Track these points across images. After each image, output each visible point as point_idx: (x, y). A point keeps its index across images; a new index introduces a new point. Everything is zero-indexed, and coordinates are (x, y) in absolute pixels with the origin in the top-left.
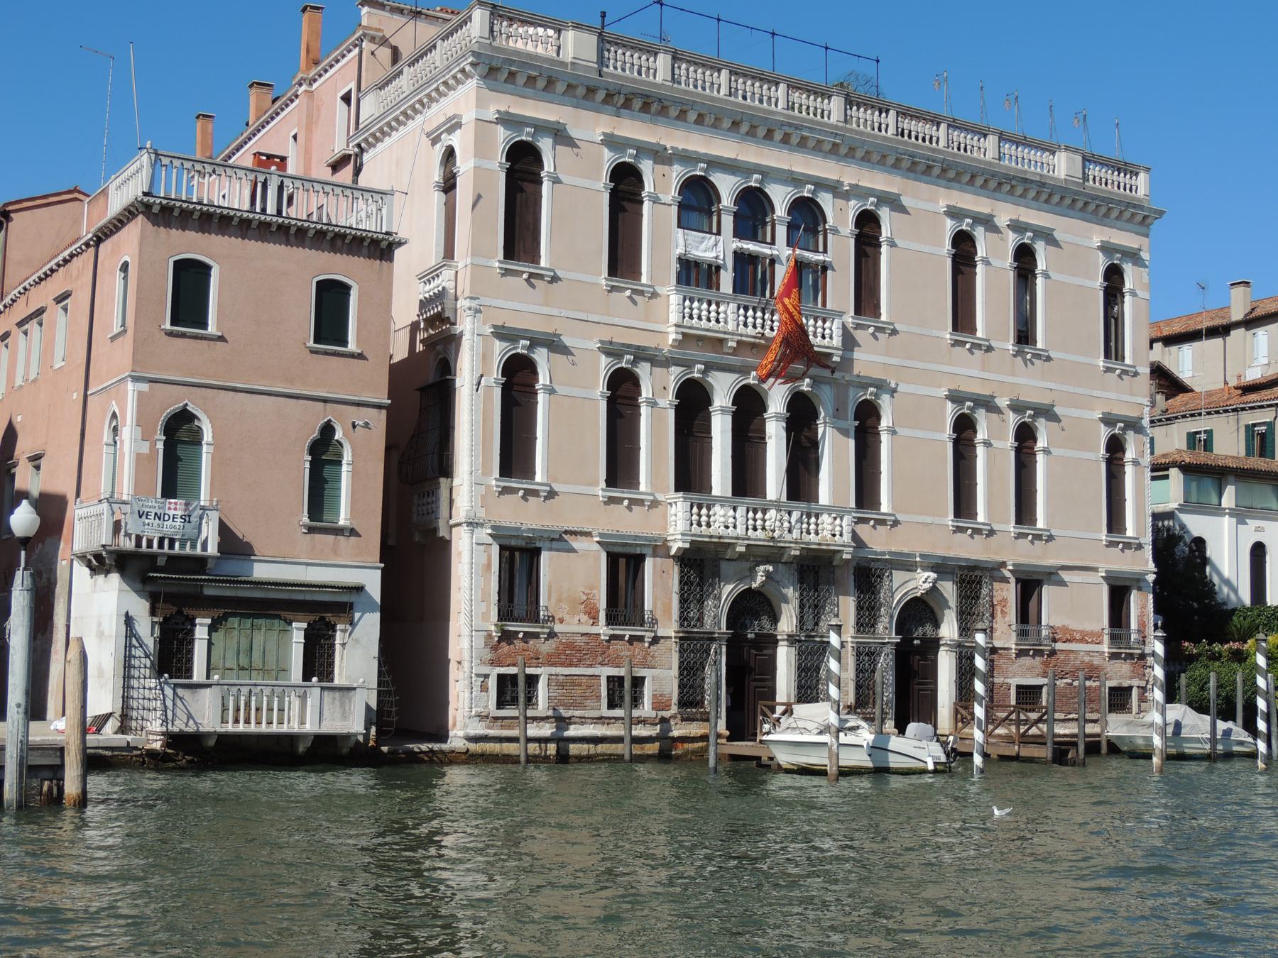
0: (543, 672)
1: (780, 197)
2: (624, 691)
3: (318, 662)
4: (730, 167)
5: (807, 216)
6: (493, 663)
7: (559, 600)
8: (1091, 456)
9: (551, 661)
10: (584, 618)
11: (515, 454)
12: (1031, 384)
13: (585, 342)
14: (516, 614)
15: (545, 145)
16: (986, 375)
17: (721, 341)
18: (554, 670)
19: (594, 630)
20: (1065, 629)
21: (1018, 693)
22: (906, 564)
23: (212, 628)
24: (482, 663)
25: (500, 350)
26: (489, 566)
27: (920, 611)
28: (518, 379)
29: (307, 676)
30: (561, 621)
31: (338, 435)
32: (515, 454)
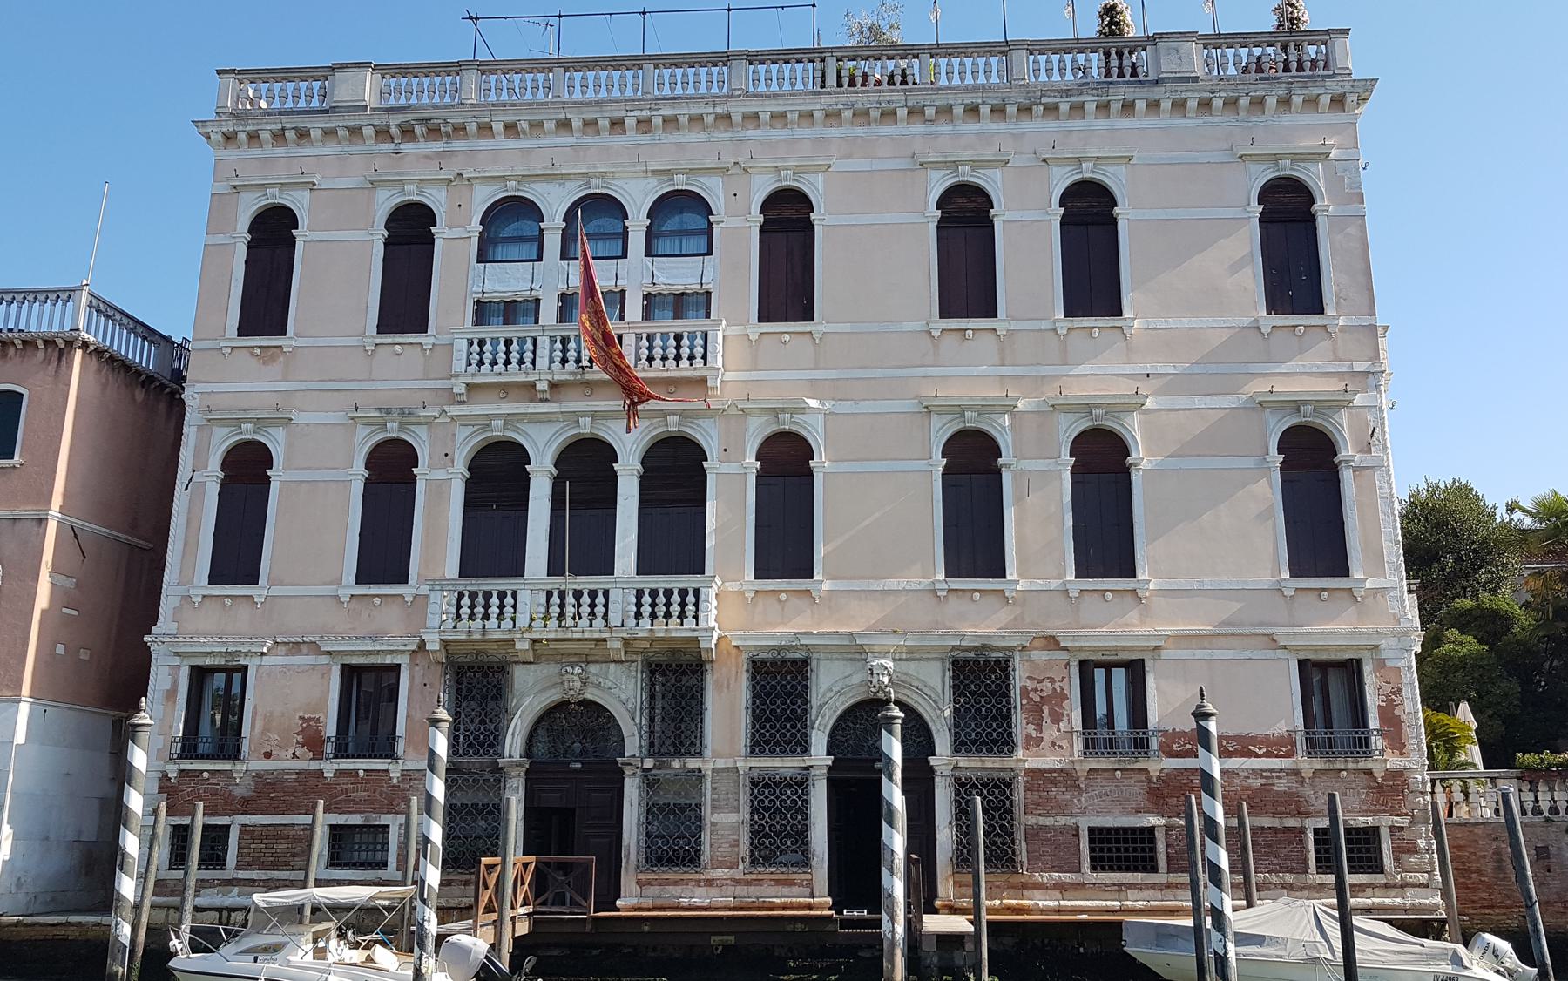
5: (681, 215)
7: (265, 730)
9: (246, 806)
10: (299, 751)
11: (237, 557)
14: (200, 751)
19: (314, 765)
22: (855, 651)
25: (222, 441)
28: (247, 469)
32: (237, 557)
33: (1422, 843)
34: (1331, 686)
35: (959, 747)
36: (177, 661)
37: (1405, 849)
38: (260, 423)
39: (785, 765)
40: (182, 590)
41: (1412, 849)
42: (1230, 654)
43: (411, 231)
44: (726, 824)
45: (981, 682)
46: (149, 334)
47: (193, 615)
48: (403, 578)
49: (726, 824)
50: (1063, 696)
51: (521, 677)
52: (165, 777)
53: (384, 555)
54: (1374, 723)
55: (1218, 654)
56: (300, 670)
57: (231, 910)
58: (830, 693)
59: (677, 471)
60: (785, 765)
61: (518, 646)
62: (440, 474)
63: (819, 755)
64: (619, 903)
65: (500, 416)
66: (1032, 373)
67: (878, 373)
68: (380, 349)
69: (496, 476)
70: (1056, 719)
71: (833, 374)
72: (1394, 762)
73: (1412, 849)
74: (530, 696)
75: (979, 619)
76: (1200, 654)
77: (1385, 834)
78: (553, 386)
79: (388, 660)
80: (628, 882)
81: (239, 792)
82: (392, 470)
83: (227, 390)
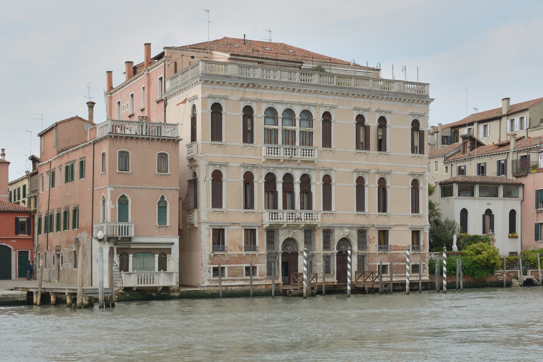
0: (226, 266)
2: (250, 271)
3: (163, 266)
4: (281, 103)
5: (307, 115)
6: (212, 264)
8: (406, 187)
9: (228, 262)
16: (368, 163)
17: (279, 160)
19: (241, 253)
20: (396, 246)
24: (209, 264)
25: (211, 169)
26: (209, 235)
28: (217, 177)
29: (159, 270)
30: (231, 251)
31: (166, 199)
36: (209, 227)
37: (424, 268)
38: (221, 165)
39: (328, 252)
43: (248, 112)
50: (374, 238)
51: (281, 232)
52: (210, 256)
54: (421, 244)
56: (236, 230)
57: (228, 286)
58: (337, 236)
60: (328, 252)
65: (271, 167)
68: (245, 148)
70: (374, 242)
74: (282, 237)
75: (361, 221)
76: (397, 229)
79: (254, 228)
81: (226, 259)
82: (248, 179)
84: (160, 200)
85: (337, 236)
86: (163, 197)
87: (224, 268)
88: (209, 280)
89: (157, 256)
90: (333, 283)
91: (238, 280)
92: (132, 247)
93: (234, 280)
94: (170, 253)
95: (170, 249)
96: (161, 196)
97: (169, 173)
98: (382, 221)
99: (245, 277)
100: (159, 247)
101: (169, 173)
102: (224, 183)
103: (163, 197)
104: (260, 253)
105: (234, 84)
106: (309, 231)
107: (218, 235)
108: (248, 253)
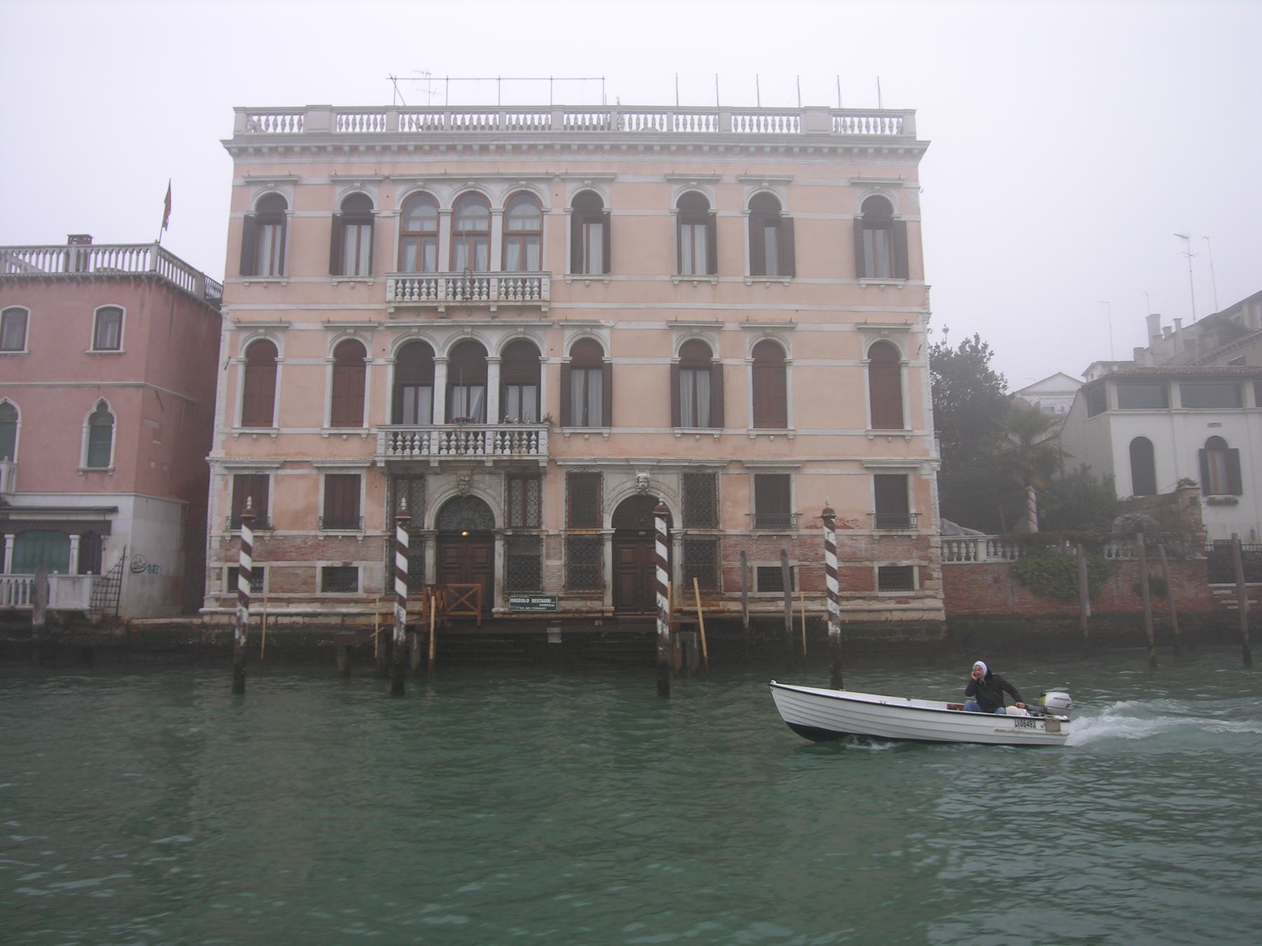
1: (497, 195)
2: (341, 578)
4: (445, 180)
8: (852, 363)
11: (258, 408)
12: (768, 304)
13: (308, 324)
15: (287, 192)
17: (436, 308)
18: (275, 564)
21: (759, 574)
22: (628, 468)
23: (15, 540)
25: (245, 340)
27: (640, 508)
28: (262, 359)
29: (82, 570)
31: (110, 409)
33: (935, 575)
34: (892, 491)
35: (686, 524)
37: (926, 576)
40: (228, 430)
41: (930, 578)
42: (837, 472)
44: (554, 566)
45: (700, 488)
46: (190, 271)
47: (230, 445)
48: (359, 423)
49: (554, 566)
53: (347, 407)
55: (831, 471)
57: (269, 615)
58: (615, 490)
59: (521, 364)
61: (432, 465)
62: (380, 361)
63: (608, 526)
64: (494, 610)
66: (735, 305)
67: (643, 306)
69: (413, 365)
71: (615, 306)
72: (924, 532)
73: (930, 578)
74: (439, 492)
75: (700, 449)
76: (822, 471)
77: (916, 570)
78: (447, 308)
80: (498, 600)
82: (349, 359)
83: (247, 307)
84: (94, 409)
85: (615, 490)
86: (102, 405)
87: (262, 569)
88: (217, 599)
89: (75, 540)
90: (602, 612)
91: (300, 601)
92: (12, 517)
93: (289, 601)
94: (109, 533)
95: (109, 522)
96: (97, 401)
97: (122, 350)
98: (768, 451)
99: (319, 594)
100: (81, 518)
101: (122, 350)
102: (280, 368)
103: (102, 405)
104: (369, 533)
105: (314, 149)
106: (524, 478)
107: (251, 488)
108: (331, 533)
